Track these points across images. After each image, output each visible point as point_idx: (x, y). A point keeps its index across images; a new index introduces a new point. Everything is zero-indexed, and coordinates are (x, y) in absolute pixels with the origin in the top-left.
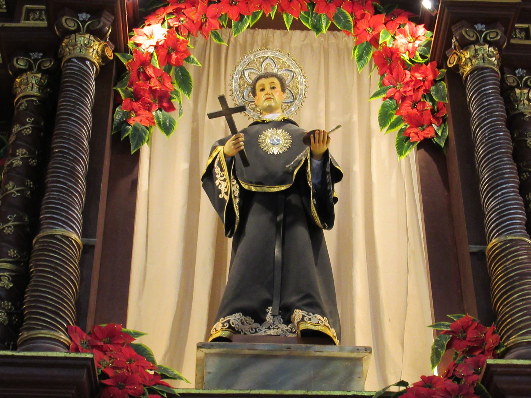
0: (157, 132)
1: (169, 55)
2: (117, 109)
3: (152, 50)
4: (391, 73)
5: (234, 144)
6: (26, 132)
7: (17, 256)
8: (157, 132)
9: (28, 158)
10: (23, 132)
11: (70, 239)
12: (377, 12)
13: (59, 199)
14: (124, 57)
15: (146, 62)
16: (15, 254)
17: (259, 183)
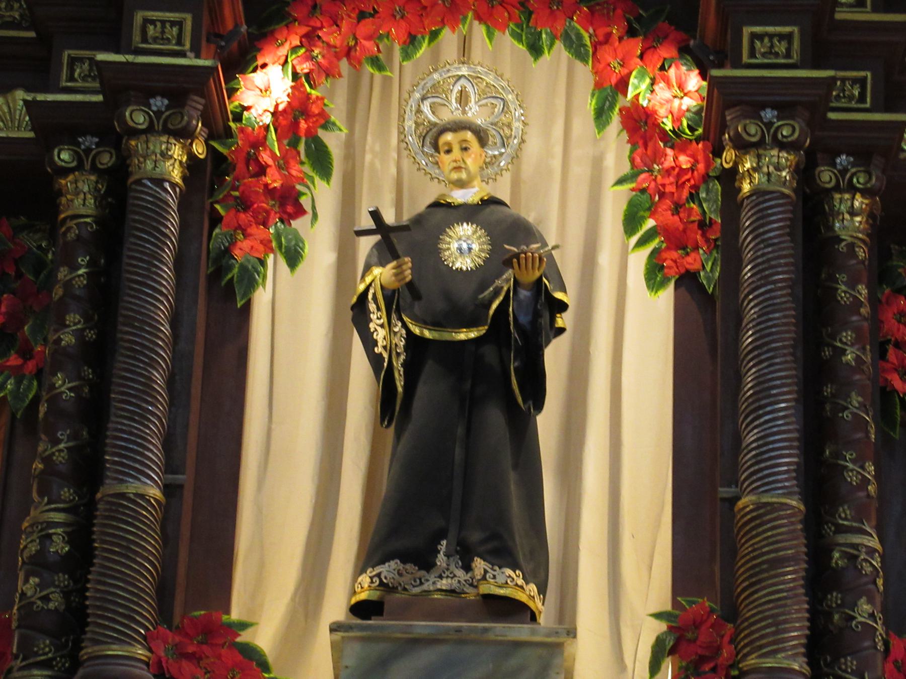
0: (275, 263)
1: (296, 124)
2: (217, 231)
3: (267, 119)
4: (646, 146)
5: (396, 275)
6: (79, 283)
7: (74, 498)
8: (275, 263)
9: (83, 330)
10: (74, 282)
11: (148, 498)
12: (632, 33)
13: (131, 434)
14: (223, 144)
15: (259, 142)
16: (71, 495)
17: (435, 324)
